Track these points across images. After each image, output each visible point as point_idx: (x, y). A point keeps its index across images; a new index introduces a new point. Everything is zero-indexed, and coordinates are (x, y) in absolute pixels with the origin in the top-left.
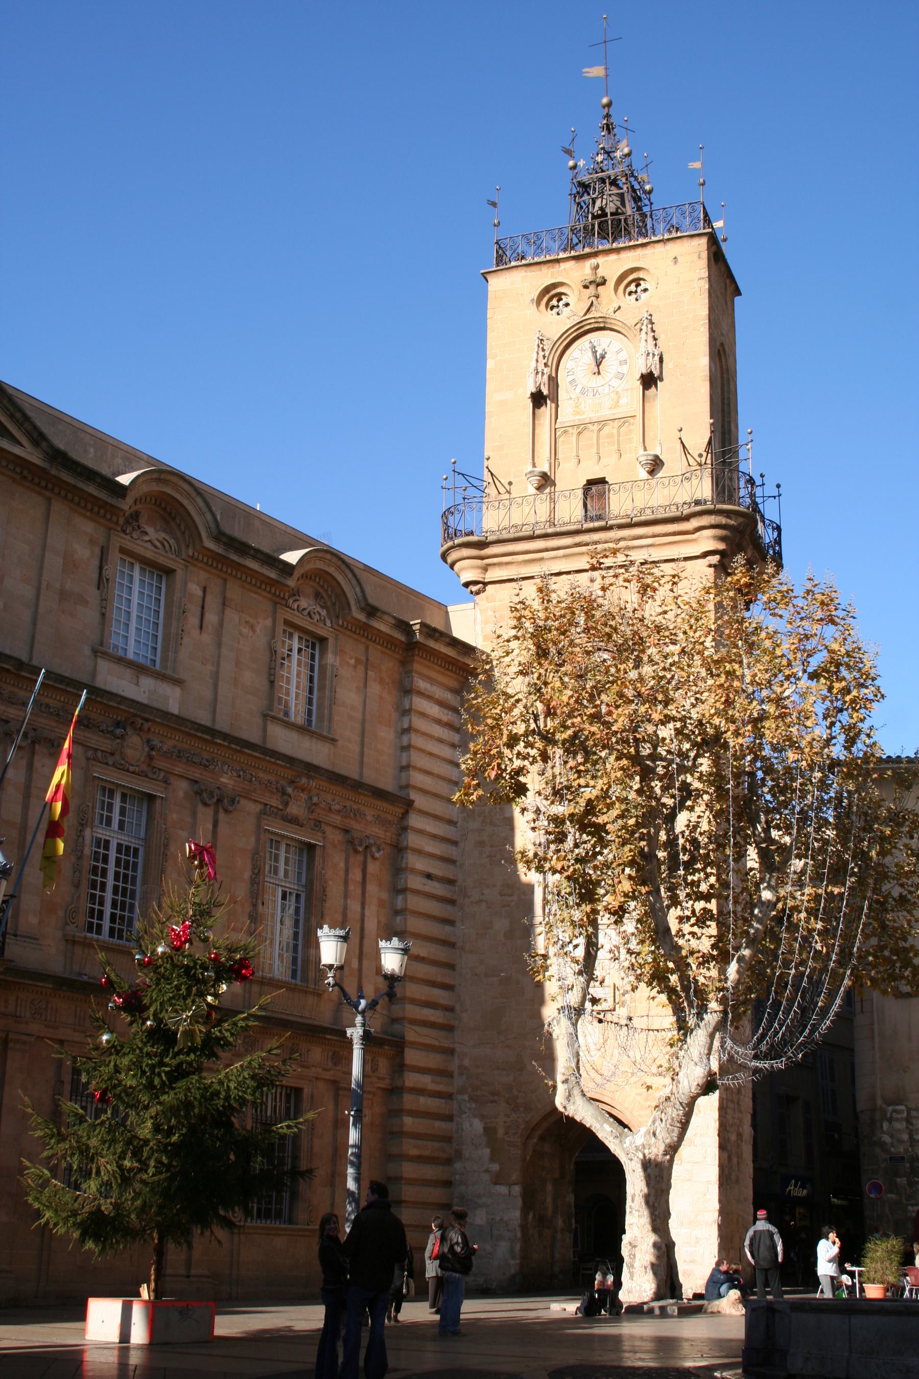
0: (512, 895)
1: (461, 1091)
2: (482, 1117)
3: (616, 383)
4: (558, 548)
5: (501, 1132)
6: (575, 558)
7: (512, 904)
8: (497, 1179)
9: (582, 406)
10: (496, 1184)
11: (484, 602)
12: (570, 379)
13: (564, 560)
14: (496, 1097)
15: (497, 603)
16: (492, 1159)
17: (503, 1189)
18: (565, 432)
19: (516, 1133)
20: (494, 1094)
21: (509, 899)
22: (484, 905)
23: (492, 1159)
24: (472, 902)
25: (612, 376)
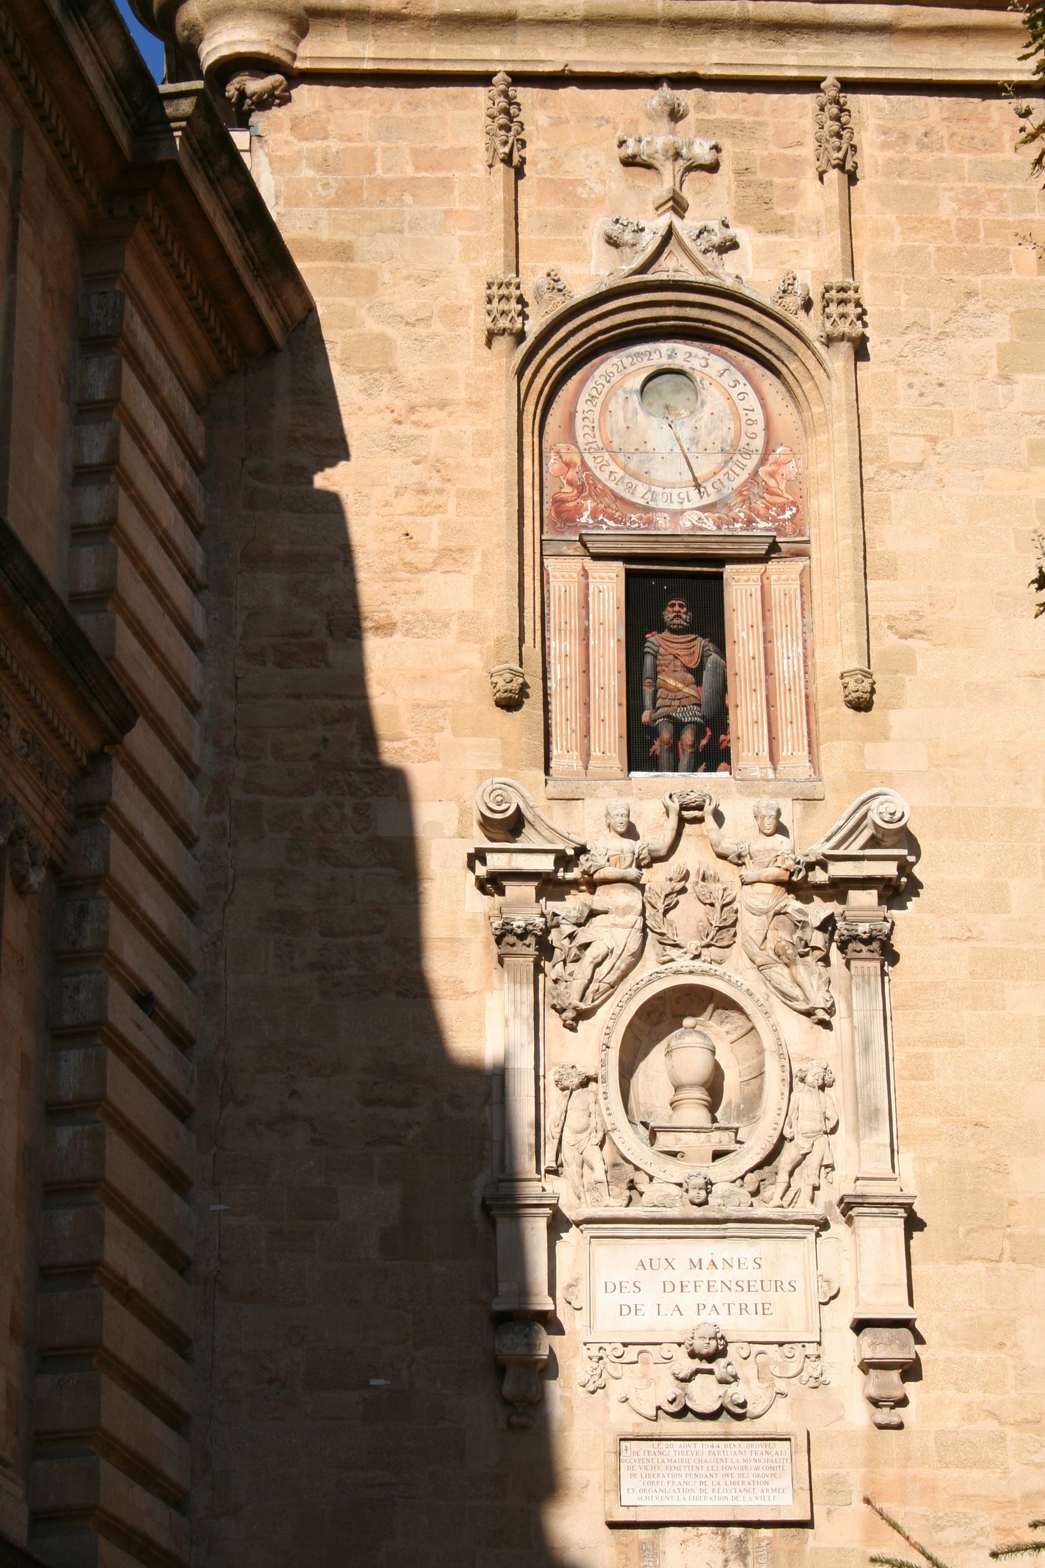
6: (621, 34)
11: (286, 135)
13: (581, 38)
15: (334, 145)
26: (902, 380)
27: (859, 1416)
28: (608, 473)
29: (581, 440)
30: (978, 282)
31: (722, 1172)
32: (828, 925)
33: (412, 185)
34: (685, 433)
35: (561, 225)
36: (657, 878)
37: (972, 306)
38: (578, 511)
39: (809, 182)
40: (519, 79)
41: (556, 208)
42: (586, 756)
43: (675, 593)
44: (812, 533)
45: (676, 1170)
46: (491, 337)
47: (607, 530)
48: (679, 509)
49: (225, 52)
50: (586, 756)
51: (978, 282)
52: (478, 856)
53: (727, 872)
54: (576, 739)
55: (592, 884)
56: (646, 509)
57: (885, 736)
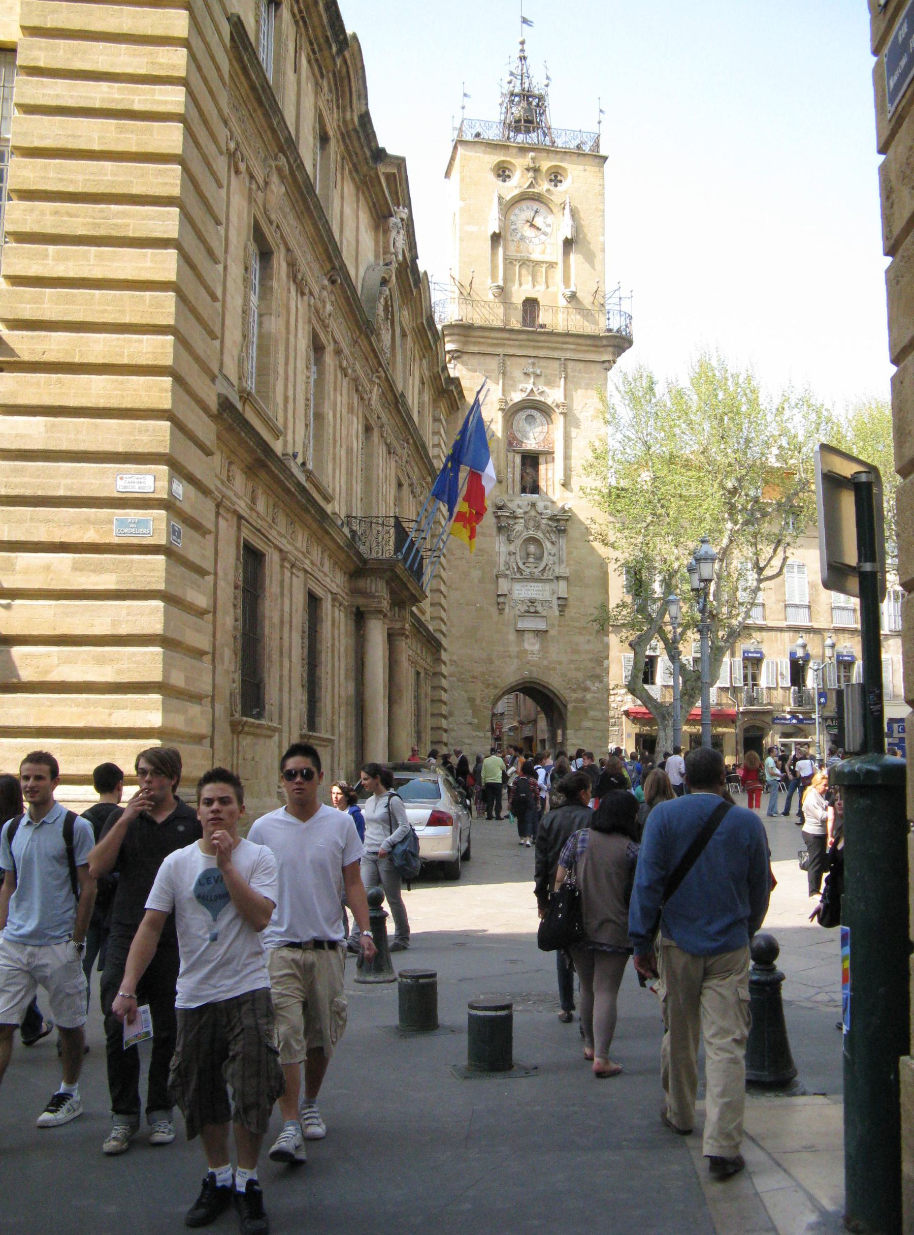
1: (452, 675)
2: (466, 691)
5: (478, 702)
8: (478, 728)
12: (513, 227)
16: (474, 717)
17: (481, 734)
18: (511, 263)
20: (474, 677)
22: (464, 561)
23: (474, 717)
27: (557, 613)
31: (535, 570)
32: (556, 527)
35: (512, 386)
36: (527, 515)
39: (558, 379)
40: (505, 355)
41: (511, 382)
44: (555, 450)
45: (528, 570)
46: (500, 409)
52: (494, 513)
53: (539, 517)
55: (516, 518)
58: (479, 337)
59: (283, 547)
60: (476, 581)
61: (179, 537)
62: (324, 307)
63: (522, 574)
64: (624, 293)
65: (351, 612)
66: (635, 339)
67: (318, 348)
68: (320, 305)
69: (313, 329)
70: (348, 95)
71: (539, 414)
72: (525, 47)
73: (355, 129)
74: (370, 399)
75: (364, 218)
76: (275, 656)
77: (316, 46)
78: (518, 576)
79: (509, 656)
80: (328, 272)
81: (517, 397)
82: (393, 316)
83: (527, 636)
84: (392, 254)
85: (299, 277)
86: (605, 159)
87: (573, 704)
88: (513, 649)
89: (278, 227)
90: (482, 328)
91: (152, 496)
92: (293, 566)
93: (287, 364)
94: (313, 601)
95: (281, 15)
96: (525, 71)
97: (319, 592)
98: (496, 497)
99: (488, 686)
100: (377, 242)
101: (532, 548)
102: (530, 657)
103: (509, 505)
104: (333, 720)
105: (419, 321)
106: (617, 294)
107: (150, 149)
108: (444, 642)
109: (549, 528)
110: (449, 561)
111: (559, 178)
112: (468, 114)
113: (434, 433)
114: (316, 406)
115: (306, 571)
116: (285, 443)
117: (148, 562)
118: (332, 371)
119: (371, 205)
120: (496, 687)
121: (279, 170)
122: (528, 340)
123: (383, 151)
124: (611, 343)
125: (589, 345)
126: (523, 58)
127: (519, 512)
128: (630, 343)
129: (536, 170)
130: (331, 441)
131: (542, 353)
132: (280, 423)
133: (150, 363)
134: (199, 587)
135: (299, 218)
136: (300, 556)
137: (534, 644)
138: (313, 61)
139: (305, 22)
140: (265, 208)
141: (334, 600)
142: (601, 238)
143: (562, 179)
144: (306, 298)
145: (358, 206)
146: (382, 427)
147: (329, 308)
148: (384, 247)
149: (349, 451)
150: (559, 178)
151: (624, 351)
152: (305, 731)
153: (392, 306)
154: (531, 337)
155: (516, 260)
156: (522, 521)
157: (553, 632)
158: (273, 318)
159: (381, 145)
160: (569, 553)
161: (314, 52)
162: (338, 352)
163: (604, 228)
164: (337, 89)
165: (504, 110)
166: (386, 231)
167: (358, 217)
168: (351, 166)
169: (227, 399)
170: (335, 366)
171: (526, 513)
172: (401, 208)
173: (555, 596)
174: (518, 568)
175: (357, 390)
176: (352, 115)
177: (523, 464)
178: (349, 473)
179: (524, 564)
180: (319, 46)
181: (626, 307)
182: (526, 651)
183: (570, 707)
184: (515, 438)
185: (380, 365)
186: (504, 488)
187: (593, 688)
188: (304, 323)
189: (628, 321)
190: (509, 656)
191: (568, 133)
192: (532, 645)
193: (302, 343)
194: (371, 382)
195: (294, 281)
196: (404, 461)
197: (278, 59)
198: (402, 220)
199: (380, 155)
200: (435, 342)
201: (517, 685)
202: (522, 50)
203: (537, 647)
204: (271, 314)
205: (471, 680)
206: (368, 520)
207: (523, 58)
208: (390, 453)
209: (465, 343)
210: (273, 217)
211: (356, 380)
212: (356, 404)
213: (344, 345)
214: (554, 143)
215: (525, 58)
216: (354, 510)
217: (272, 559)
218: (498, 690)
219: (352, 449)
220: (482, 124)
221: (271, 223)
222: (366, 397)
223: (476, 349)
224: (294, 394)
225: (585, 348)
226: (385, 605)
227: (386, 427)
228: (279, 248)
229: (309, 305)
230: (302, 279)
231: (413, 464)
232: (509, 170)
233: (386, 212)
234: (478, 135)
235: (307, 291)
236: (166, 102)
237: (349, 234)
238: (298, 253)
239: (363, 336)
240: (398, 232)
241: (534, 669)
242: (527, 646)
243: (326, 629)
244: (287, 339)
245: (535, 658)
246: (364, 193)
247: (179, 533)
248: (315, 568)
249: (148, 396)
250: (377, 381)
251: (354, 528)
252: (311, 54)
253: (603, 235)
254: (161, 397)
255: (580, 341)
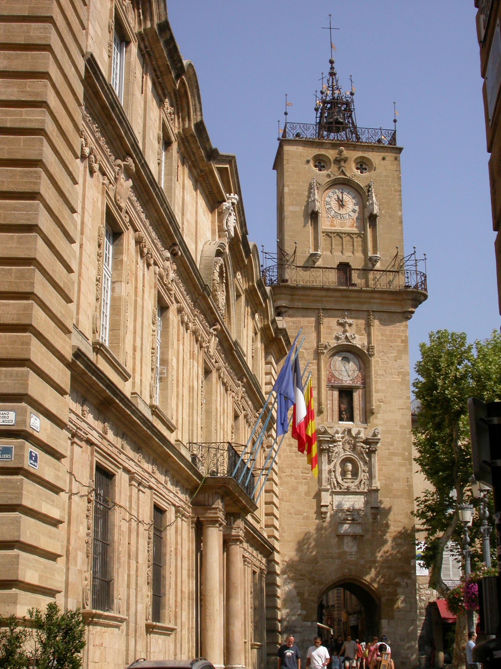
0: (308, 473)
3: (352, 214)
4: (332, 297)
5: (306, 595)
7: (308, 478)
9: (335, 222)
10: (304, 621)
12: (328, 206)
14: (303, 577)
19: (314, 596)
21: (308, 475)
24: (286, 476)
25: (350, 210)
26: (380, 361)
27: (371, 520)
28: (336, 374)
29: (332, 368)
30: (392, 344)
31: (352, 484)
32: (368, 448)
33: (307, 326)
34: (347, 367)
36: (344, 440)
37: (391, 349)
38: (332, 380)
42: (333, 419)
43: (346, 393)
47: (336, 384)
48: (347, 381)
49: (279, 305)
50: (333, 419)
51: (392, 344)
54: (331, 417)
55: (335, 441)
56: (341, 380)
57: (377, 418)
58: (303, 295)
59: (131, 469)
60: (303, 495)
61: (36, 461)
62: (168, 275)
63: (341, 488)
64: (419, 256)
65: (192, 523)
66: (429, 294)
67: (162, 308)
68: (164, 273)
69: (159, 292)
70: (186, 109)
71: (352, 356)
72: (334, 65)
73: (192, 135)
74: (208, 347)
75: (202, 203)
76: (124, 559)
77: (158, 73)
78: (338, 490)
79: (332, 557)
80: (171, 247)
81: (334, 343)
82: (227, 280)
83: (346, 540)
84: (225, 232)
85: (145, 250)
86: (400, 150)
87: (386, 597)
88: (335, 551)
89: (127, 212)
90: (304, 288)
91: (13, 428)
92: (140, 484)
93: (135, 320)
94: (159, 511)
95: (131, 50)
96: (335, 84)
97: (163, 505)
98: (319, 424)
99: (314, 583)
100: (213, 222)
101: (349, 466)
102: (349, 558)
103: (329, 431)
104: (176, 612)
105: (251, 284)
106: (413, 257)
107: (18, 156)
108: (277, 545)
109: (362, 449)
110: (280, 478)
111: (364, 167)
112: (290, 119)
113: (267, 374)
114: (162, 353)
115: (150, 488)
116: (134, 383)
117: (9, 481)
118: (176, 325)
119: (207, 193)
120: (320, 583)
121: (127, 169)
122: (343, 297)
123: (216, 151)
124: (410, 297)
125: (392, 300)
126: (332, 74)
127: (338, 436)
128: (426, 297)
129: (345, 160)
130: (175, 381)
131: (353, 307)
132: (129, 369)
133: (15, 322)
134: (53, 501)
135: (145, 205)
136: (147, 475)
137: (352, 547)
138: (157, 84)
139: (149, 55)
140: (115, 198)
141: (177, 511)
142: (399, 213)
143: (366, 167)
144: (152, 268)
145: (197, 194)
146: (218, 370)
147: (172, 275)
148: (219, 226)
149: (191, 389)
150: (364, 167)
151: (420, 303)
152: (150, 622)
153: (226, 273)
154: (344, 294)
155: (331, 233)
156: (341, 443)
157: (368, 537)
158: (123, 284)
159: (214, 146)
160: (380, 470)
161: (158, 78)
162: (180, 311)
163: (401, 205)
164: (177, 104)
165: (319, 115)
166: (220, 214)
167: (197, 203)
168: (190, 163)
169: (79, 350)
170: (178, 321)
171: (342, 438)
172: (232, 194)
173: (369, 506)
174: (338, 483)
175: (197, 341)
176: (189, 124)
177: (340, 396)
178: (191, 407)
179: (342, 480)
180: (161, 72)
181: (421, 268)
182: (346, 553)
183: (383, 599)
184: (333, 376)
185: (217, 320)
186: (325, 418)
187: (403, 584)
188: (151, 287)
189: (423, 279)
190: (332, 557)
191: (370, 130)
192: (350, 547)
193: (150, 304)
194: (209, 333)
195: (142, 256)
196: (240, 397)
197: (128, 83)
198: (233, 204)
199: (213, 155)
200: (265, 301)
201: (338, 582)
202: (332, 68)
203: (355, 549)
204: (121, 281)
205: (301, 577)
206: (208, 446)
207: (332, 74)
208: (227, 390)
209: (292, 300)
210: (123, 205)
211: (195, 332)
212: (196, 351)
213: (184, 305)
214: (358, 138)
215: (335, 74)
216: (195, 437)
217: (121, 478)
218: (322, 586)
219: (193, 388)
220: (302, 125)
221: (121, 209)
222: (204, 345)
223: (300, 305)
224: (142, 344)
225: (389, 302)
226: (221, 515)
227: (223, 369)
228: (128, 229)
229: (155, 274)
230: (148, 253)
231: (247, 399)
232: (324, 162)
233: (220, 199)
234: (298, 135)
235: (152, 262)
236: (31, 121)
237: (190, 216)
238: (143, 233)
239: (200, 297)
240: (230, 214)
241: (351, 567)
242: (346, 549)
243: (170, 534)
244: (136, 301)
245: (354, 558)
246: (201, 184)
247: (36, 457)
248: (160, 485)
249: (13, 348)
250: (215, 333)
251: (195, 452)
252: (155, 78)
253: (401, 210)
254: (23, 349)
255: (385, 296)
